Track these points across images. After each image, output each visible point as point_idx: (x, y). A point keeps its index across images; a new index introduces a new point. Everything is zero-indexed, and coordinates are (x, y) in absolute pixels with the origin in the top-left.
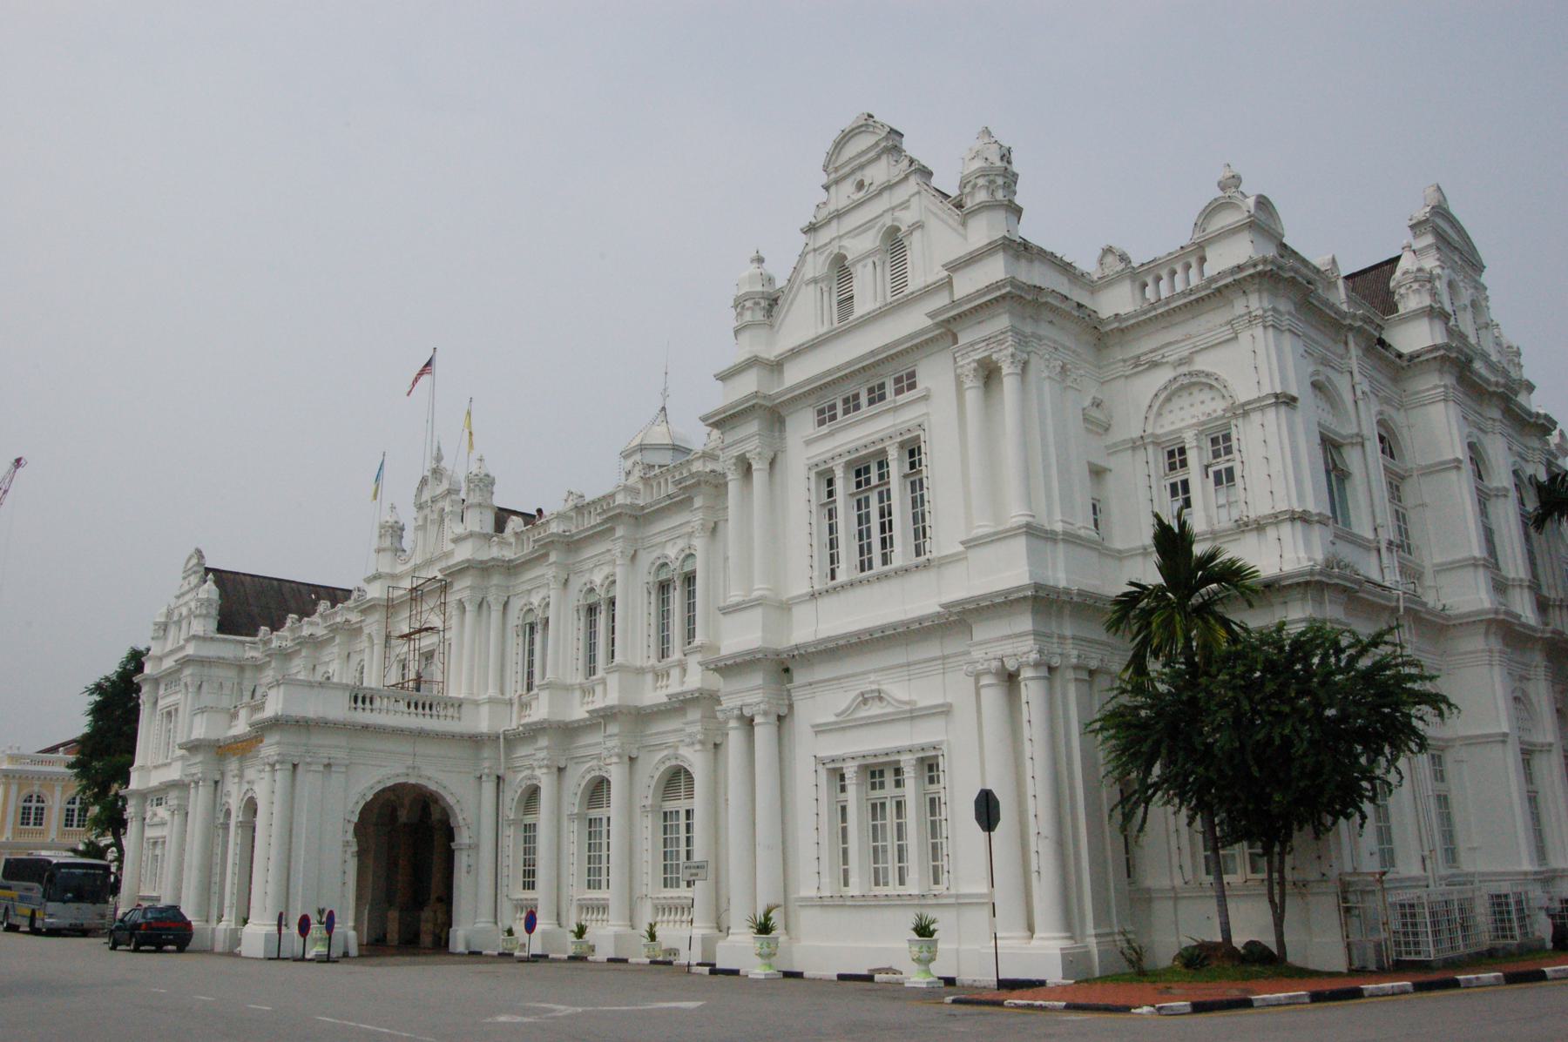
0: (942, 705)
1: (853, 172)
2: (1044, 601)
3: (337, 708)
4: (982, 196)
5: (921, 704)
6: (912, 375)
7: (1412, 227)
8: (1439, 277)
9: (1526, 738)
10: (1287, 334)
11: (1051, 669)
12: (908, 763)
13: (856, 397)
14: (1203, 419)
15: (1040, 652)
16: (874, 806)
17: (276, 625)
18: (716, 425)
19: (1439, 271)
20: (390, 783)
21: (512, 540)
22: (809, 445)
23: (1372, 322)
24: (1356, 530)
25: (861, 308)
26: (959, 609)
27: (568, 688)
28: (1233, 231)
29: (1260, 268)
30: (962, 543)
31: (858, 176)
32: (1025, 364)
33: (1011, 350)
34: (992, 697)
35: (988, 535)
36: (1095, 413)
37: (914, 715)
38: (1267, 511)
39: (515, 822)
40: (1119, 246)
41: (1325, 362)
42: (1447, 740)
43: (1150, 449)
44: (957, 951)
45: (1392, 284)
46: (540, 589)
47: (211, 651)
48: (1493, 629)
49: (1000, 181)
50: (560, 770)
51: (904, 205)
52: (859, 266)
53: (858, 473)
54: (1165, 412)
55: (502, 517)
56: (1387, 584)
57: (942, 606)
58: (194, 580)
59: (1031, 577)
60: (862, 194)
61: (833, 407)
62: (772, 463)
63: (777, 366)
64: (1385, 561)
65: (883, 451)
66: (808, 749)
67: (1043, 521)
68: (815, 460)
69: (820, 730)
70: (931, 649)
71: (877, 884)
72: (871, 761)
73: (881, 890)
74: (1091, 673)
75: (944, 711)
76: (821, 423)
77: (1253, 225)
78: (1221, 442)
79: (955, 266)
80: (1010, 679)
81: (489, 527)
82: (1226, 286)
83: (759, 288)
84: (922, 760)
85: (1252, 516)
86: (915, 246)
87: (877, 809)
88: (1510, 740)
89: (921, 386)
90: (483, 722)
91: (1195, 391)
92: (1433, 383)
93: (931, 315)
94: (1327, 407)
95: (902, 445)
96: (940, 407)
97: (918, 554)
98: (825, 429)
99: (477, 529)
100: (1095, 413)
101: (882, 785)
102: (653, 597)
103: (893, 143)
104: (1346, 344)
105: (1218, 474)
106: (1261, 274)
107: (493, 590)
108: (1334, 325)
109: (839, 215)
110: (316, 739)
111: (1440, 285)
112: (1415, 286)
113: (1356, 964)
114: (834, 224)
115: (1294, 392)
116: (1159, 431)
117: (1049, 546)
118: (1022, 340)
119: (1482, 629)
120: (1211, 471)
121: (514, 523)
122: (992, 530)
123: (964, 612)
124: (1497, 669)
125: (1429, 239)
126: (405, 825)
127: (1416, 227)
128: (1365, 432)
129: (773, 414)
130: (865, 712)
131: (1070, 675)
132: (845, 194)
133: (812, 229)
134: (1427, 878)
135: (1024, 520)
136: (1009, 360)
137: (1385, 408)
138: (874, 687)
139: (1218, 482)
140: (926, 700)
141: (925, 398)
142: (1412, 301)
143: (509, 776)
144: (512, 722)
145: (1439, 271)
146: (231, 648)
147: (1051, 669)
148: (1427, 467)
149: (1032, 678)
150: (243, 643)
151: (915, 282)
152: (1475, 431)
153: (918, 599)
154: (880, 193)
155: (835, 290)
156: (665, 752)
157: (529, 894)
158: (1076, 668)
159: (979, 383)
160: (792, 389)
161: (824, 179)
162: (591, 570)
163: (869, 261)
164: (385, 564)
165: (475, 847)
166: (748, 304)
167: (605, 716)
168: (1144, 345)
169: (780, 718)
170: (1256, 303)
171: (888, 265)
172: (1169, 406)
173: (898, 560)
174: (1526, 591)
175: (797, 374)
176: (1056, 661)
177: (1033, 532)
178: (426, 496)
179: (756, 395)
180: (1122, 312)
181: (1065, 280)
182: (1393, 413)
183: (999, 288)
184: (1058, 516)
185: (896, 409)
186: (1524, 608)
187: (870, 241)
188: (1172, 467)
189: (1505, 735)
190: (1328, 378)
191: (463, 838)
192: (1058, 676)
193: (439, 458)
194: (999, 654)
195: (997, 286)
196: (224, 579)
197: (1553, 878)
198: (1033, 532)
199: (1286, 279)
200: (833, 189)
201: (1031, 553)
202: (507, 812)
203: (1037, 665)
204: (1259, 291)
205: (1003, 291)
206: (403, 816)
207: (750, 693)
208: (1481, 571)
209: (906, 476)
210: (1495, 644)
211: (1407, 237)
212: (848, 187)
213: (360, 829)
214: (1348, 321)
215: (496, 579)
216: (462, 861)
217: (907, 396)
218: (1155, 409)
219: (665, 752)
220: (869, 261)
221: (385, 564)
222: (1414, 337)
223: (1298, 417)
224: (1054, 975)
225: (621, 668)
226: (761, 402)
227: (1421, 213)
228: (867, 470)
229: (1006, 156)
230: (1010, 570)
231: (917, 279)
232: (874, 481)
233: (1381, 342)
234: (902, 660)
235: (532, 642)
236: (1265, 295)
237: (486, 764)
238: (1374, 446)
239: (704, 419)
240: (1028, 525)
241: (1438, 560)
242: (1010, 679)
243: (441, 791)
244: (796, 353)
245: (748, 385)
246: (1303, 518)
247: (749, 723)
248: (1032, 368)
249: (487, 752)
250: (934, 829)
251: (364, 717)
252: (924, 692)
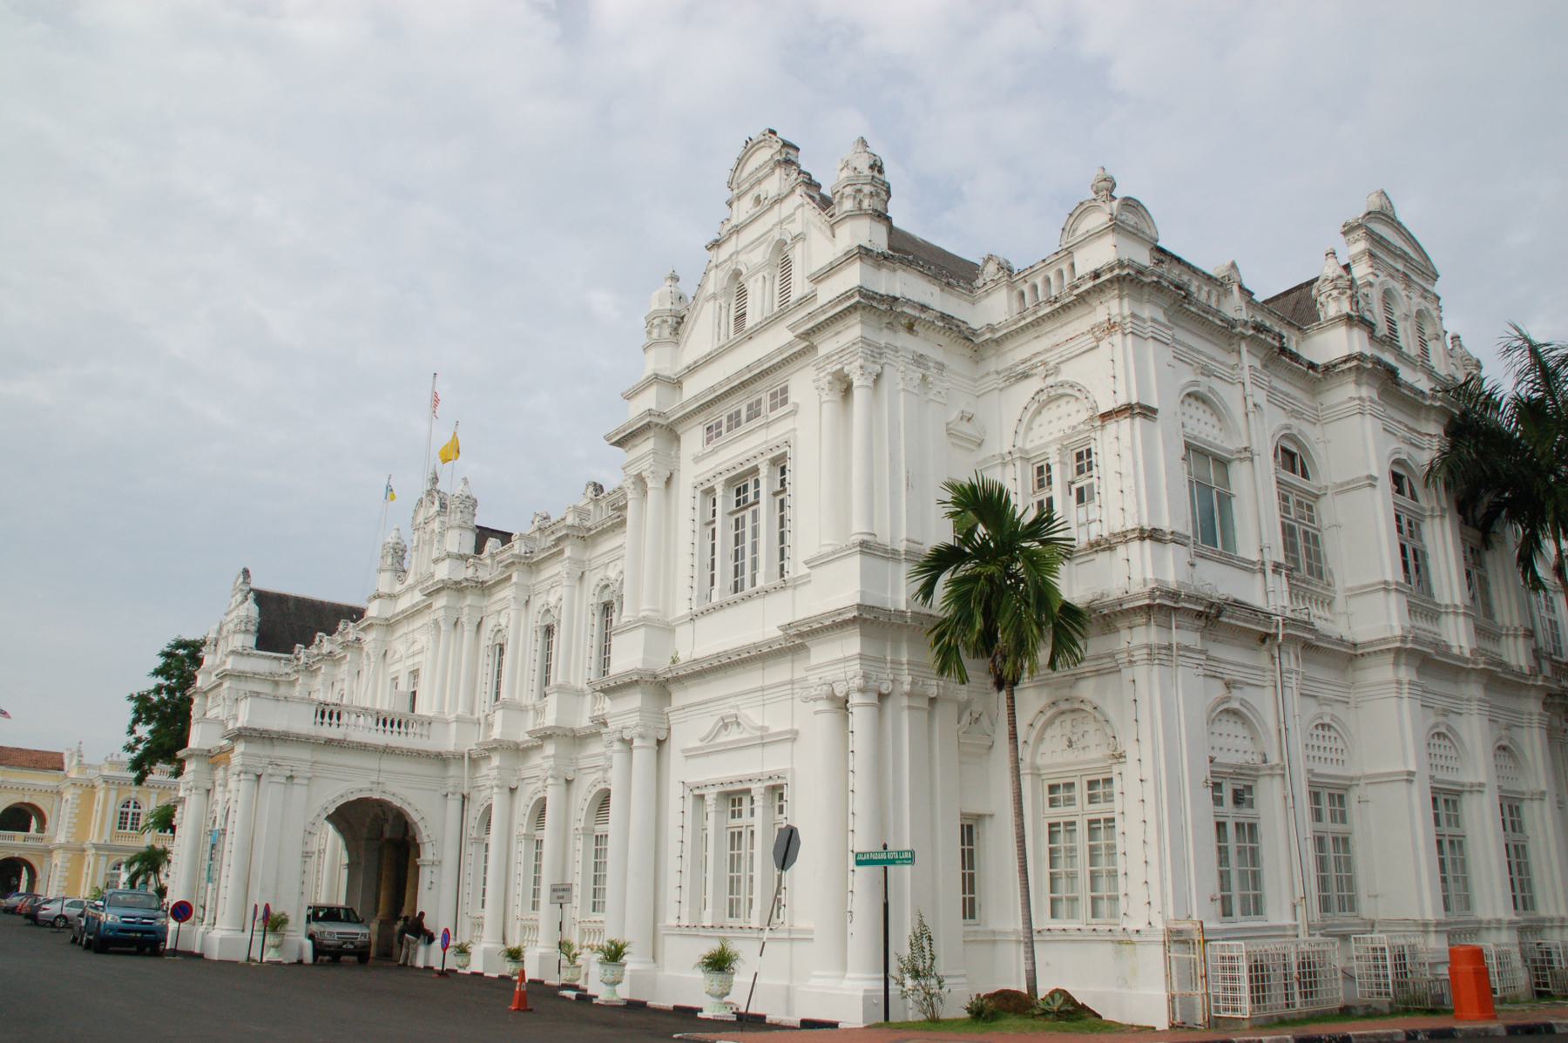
0: (786, 732)
1: (752, 187)
2: (870, 621)
3: (302, 722)
4: (848, 205)
5: (774, 729)
6: (785, 390)
7: (1345, 233)
8: (1371, 284)
9: (1440, 775)
10: (1151, 343)
11: (882, 697)
12: (758, 789)
13: (738, 413)
14: (1069, 432)
15: (865, 677)
16: (733, 834)
17: (308, 643)
18: (620, 443)
19: (1371, 278)
20: (352, 798)
21: (488, 561)
22: (701, 460)
23: (1268, 330)
24: (1241, 553)
25: (750, 322)
26: (792, 632)
27: (522, 709)
28: (1099, 234)
29: (1116, 272)
30: (806, 563)
31: (755, 192)
32: (879, 376)
33: (860, 361)
35: (828, 555)
36: (966, 428)
37: (765, 740)
38: (1118, 529)
39: (478, 841)
40: (1002, 254)
41: (1206, 372)
42: (1352, 779)
43: (1018, 463)
44: (788, 988)
45: (1314, 292)
46: (506, 613)
47: (247, 665)
48: (1403, 659)
49: (867, 189)
50: (512, 790)
51: (790, 218)
52: (751, 281)
53: (738, 493)
54: (1035, 426)
55: (483, 534)
56: (1270, 609)
57: (780, 628)
58: (239, 597)
59: (863, 593)
61: (719, 425)
62: (669, 481)
64: (1270, 584)
65: (755, 470)
66: (682, 771)
67: (885, 538)
68: (701, 479)
69: (690, 754)
70: (780, 673)
71: (731, 916)
72: (730, 788)
73: (730, 922)
74: (932, 701)
75: (793, 736)
76: (709, 440)
77: (1116, 226)
78: (1084, 460)
79: (818, 278)
80: (843, 705)
81: (469, 549)
82: (1088, 292)
83: (669, 306)
84: (774, 788)
85: (1105, 534)
86: (797, 255)
87: (736, 837)
88: (1416, 779)
89: (791, 400)
90: (449, 741)
91: (1063, 402)
92: (1348, 392)
93: (792, 328)
94: (1214, 420)
95: (774, 462)
96: (807, 423)
97: (782, 576)
98: (710, 448)
99: (454, 549)
100: (966, 428)
101: (740, 815)
102: (597, 618)
103: (788, 156)
104: (1239, 352)
105: (1080, 491)
106: (1119, 280)
107: (466, 611)
108: (1227, 332)
109: (737, 230)
110: (280, 751)
111: (1375, 295)
112: (1335, 293)
113: (1178, 1019)
114: (734, 237)
115: (1155, 405)
116: (1029, 446)
117: (890, 564)
118: (875, 353)
119: (1390, 658)
120: (1074, 488)
121: (492, 544)
122: (829, 549)
123: (800, 635)
124: (1406, 703)
125: (1362, 245)
126: (388, 840)
127: (1348, 230)
128: (1254, 447)
130: (724, 738)
131: (905, 702)
132: (745, 208)
133: (716, 244)
134: (1296, 927)
135: (857, 539)
136: (859, 372)
137: (1293, 422)
138: (733, 711)
139: (1080, 499)
140: (778, 726)
141: (794, 413)
142: (1333, 307)
143: (474, 795)
144: (470, 742)
145: (1371, 278)
146: (265, 663)
147: (882, 697)
148: (1341, 485)
149: (858, 705)
150: (280, 659)
151: (796, 294)
152: (1405, 447)
153: (758, 623)
154: (772, 205)
155: (733, 306)
156: (594, 776)
157: (532, 915)
158: (910, 695)
159: (838, 397)
160: (683, 406)
161: (728, 195)
162: (548, 591)
163: (760, 276)
164: (385, 583)
165: (437, 864)
166: (656, 322)
167: (546, 736)
168: (1018, 353)
169: (660, 743)
170: (1113, 307)
171: (777, 279)
172: (1039, 420)
173: (760, 582)
174: (1461, 619)
175: (695, 388)
176: (884, 691)
177: (867, 548)
178: (420, 519)
179: (650, 412)
180: (995, 322)
181: (936, 290)
182: (1306, 427)
183: (849, 298)
185: (768, 425)
186: (1458, 635)
187: (759, 256)
188: (1041, 485)
189: (1411, 773)
190: (1210, 389)
191: (427, 854)
192: (889, 706)
193: (435, 480)
195: (846, 296)
196: (262, 598)
197: (1479, 930)
198: (867, 548)
199: (1167, 288)
200: (735, 205)
201: (865, 575)
202: (470, 831)
203: (863, 691)
204: (1121, 297)
205: (853, 301)
206: (387, 834)
207: (627, 712)
208: (1393, 596)
209: (776, 494)
210: (1406, 674)
211: (1339, 243)
214: (1239, 329)
215: (469, 600)
216: (425, 876)
217: (781, 411)
218: (1026, 420)
219: (594, 776)
220: (760, 276)
221: (385, 583)
222: (1332, 343)
223: (1158, 429)
224: (852, 1017)
225: (561, 689)
226: (656, 420)
227: (1357, 213)
228: (746, 487)
229: (877, 167)
230: (841, 588)
231: (796, 294)
232: (751, 499)
233: (1283, 350)
234: (758, 684)
235: (500, 664)
236: (1126, 301)
237: (451, 782)
238: (1267, 464)
239: (607, 438)
240: (864, 544)
241: (1349, 585)
242: (843, 705)
243: (406, 807)
244: (692, 369)
245: (649, 400)
246: (1153, 535)
247: (628, 743)
248: (885, 384)
249: (453, 770)
250: (734, 862)
251: (330, 731)
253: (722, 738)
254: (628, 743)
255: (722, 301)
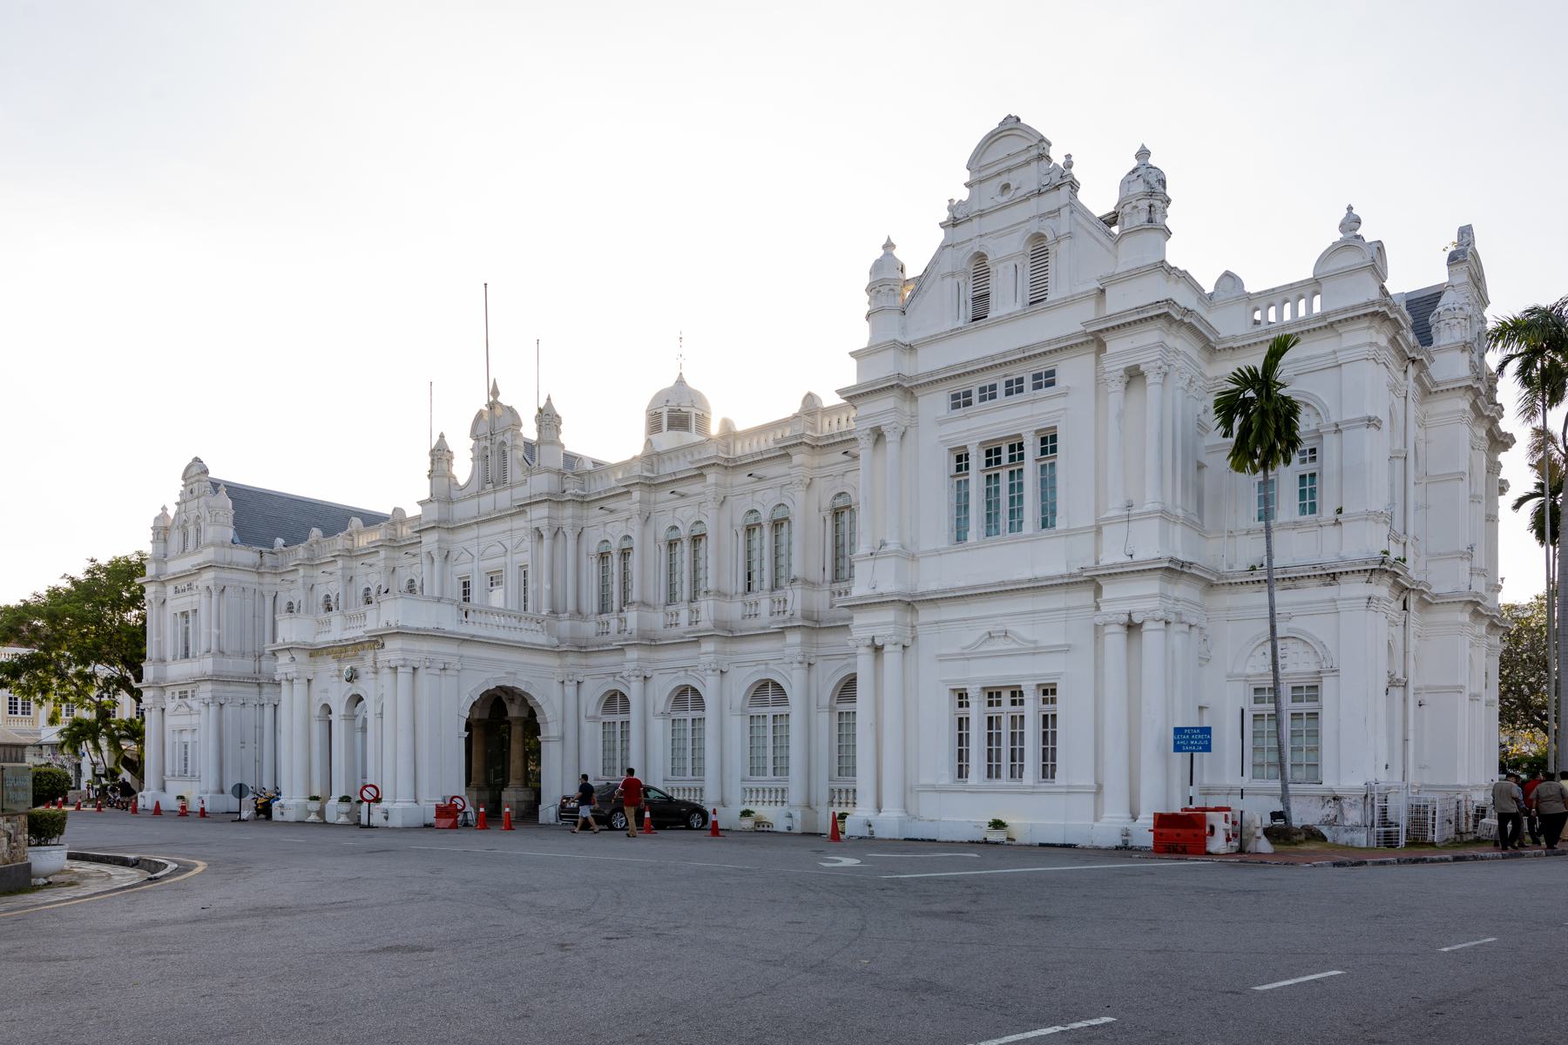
31: (1004, 179)
34: (1115, 640)
37: (1036, 651)
52: (1000, 267)
60: (1005, 199)
63: (911, 348)
69: (942, 658)
75: (1067, 649)
129: (906, 389)
166: (884, 289)
184: (1179, 502)
194: (1127, 609)
212: (994, 186)
213: (469, 726)
247: (878, 650)
252: (1050, 635)
253: (983, 648)
254: (878, 650)
255: (960, 280)
